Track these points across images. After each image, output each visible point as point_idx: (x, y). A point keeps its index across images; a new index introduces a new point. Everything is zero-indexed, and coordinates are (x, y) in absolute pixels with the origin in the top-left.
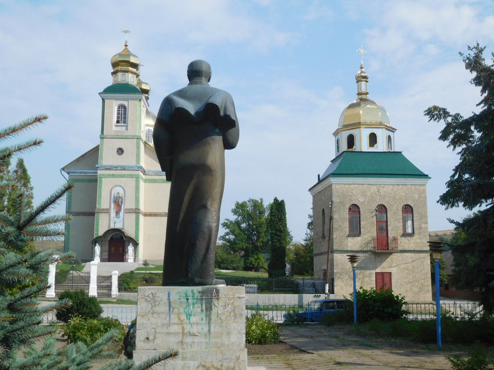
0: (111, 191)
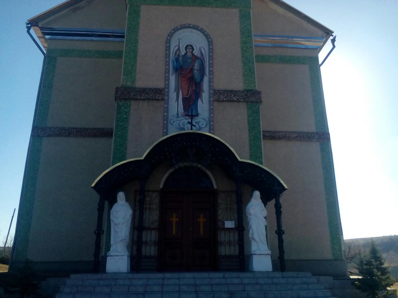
0: (168, 41)
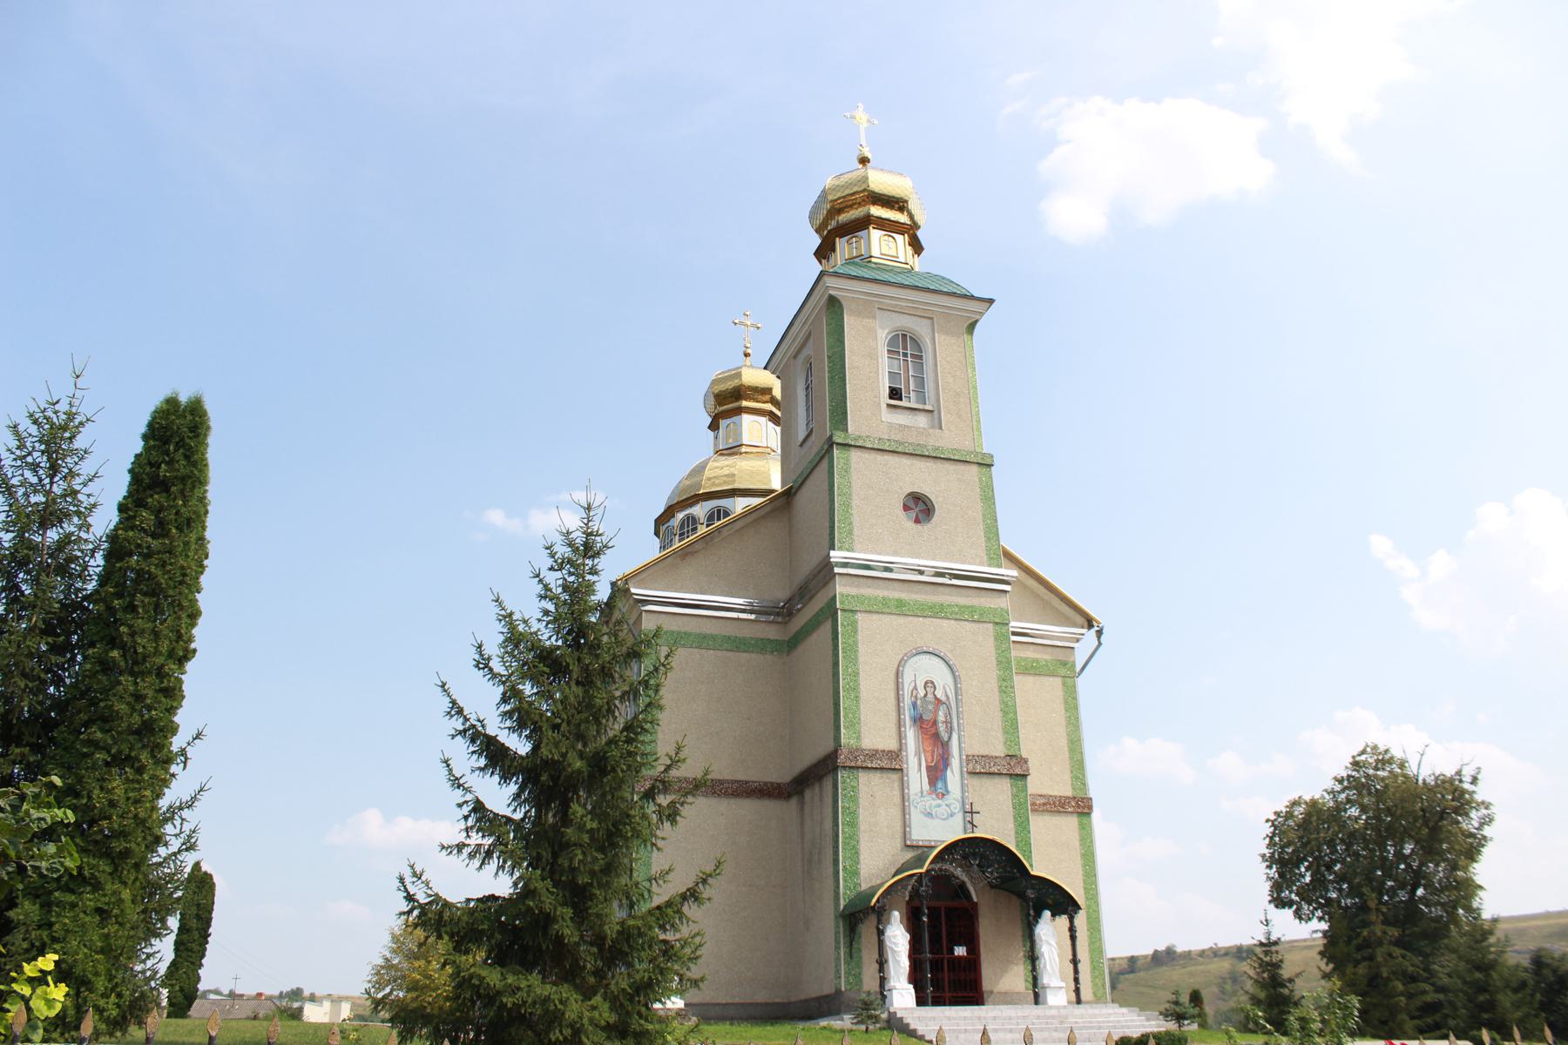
0: (898, 675)
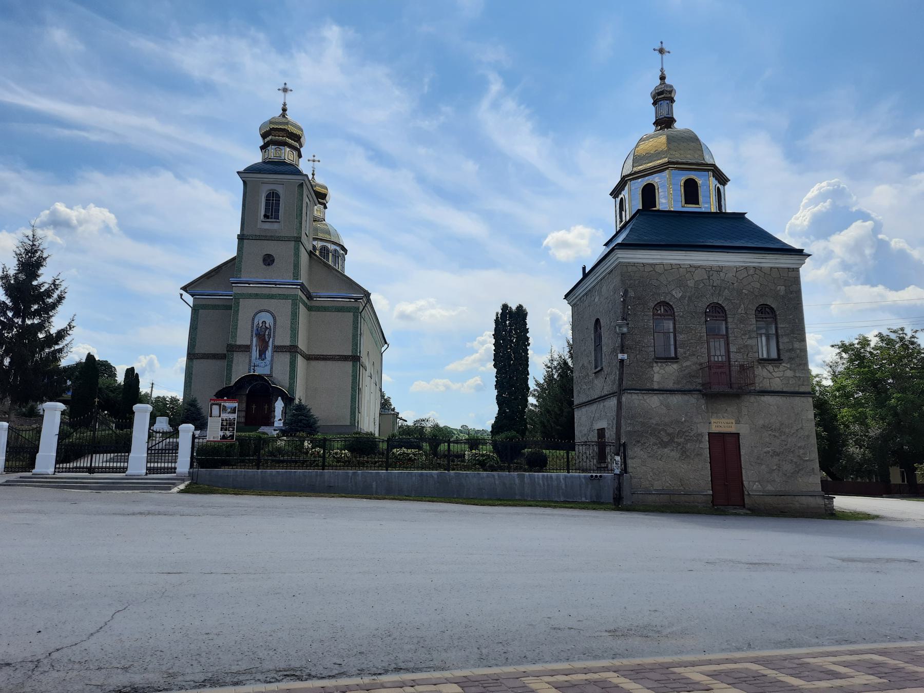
0: (253, 319)
